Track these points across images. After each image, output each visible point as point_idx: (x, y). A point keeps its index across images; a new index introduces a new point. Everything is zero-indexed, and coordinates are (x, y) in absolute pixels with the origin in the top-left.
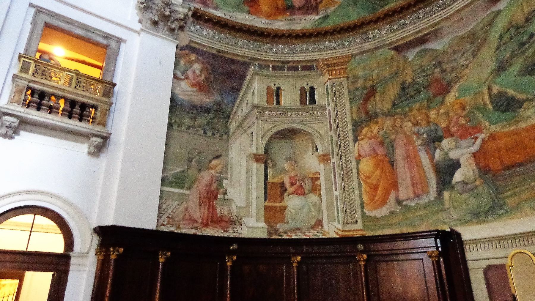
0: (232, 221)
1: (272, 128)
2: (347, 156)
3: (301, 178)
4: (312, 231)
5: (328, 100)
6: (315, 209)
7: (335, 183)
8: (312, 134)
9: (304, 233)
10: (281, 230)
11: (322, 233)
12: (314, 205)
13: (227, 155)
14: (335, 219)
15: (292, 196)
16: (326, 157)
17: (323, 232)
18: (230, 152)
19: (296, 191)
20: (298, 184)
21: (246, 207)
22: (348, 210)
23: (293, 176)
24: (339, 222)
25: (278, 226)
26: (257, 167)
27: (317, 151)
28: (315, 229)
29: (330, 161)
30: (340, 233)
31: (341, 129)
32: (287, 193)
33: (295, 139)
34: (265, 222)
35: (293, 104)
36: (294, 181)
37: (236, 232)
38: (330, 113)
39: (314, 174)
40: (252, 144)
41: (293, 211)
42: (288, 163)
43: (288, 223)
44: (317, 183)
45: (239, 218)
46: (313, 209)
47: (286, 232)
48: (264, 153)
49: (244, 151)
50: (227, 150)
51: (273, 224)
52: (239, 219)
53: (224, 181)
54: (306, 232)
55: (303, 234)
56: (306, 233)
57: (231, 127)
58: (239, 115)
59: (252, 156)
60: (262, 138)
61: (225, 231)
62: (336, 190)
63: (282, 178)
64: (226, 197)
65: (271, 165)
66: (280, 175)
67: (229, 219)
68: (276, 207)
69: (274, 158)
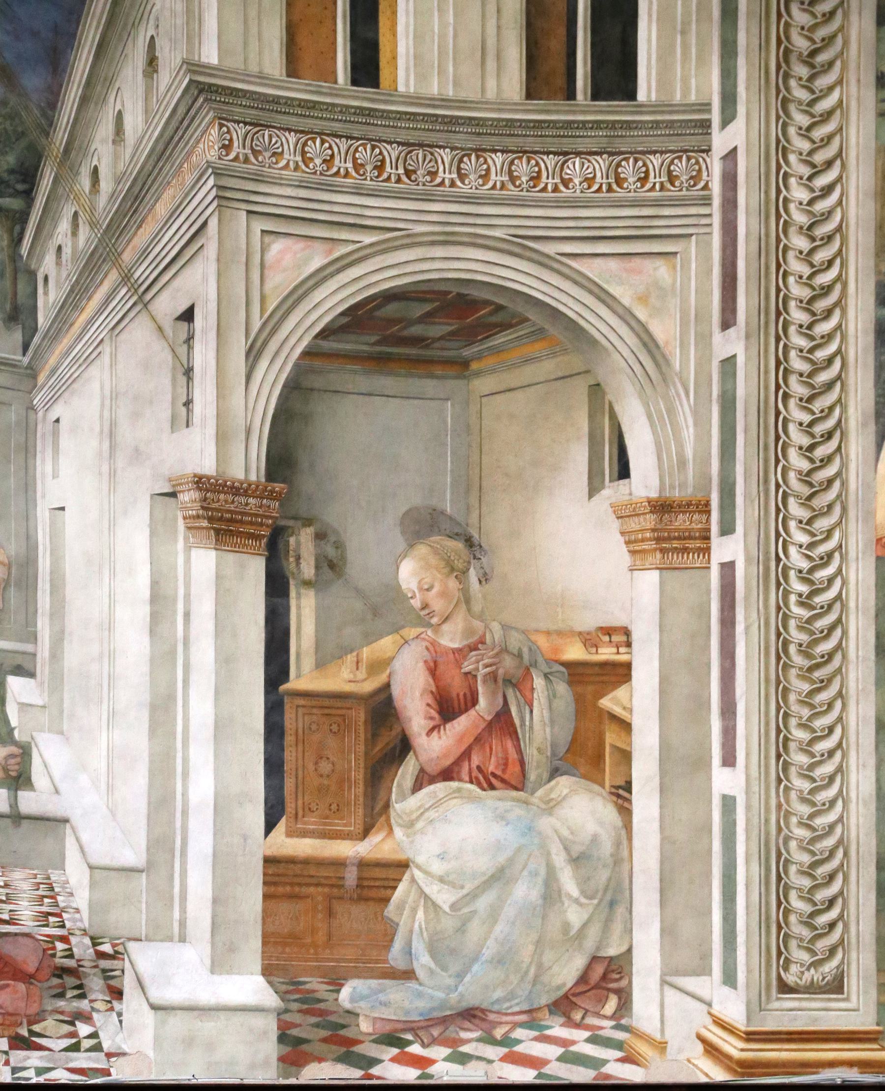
0: (62, 972)
1: (320, 277)
2: (823, 524)
3: (508, 662)
4: (558, 1031)
5: (728, 75)
6: (583, 882)
7: (728, 710)
8: (594, 342)
9: (506, 1041)
10: (365, 1026)
11: (619, 1045)
12: (577, 860)
13: (28, 487)
14: (706, 957)
15: (440, 788)
16: (681, 522)
17: (620, 1035)
18: (43, 465)
19: (466, 754)
20: (484, 706)
21: (149, 868)
22: (796, 903)
23: (454, 651)
24: (729, 979)
25: (345, 994)
26: (219, 577)
27: (624, 472)
28: (577, 1016)
29: (707, 550)
30: (733, 1047)
31: (798, 316)
32: (408, 770)
33: (478, 374)
34: (267, 972)
35: (470, 93)
36: (457, 687)
37: (92, 1042)
38: (730, 180)
39: (589, 640)
40: (188, 403)
41: (444, 897)
42: (422, 549)
43: (409, 975)
44: (606, 703)
45: (107, 948)
46: (569, 883)
47: (391, 1039)
48: (270, 476)
49: (137, 455)
50: (28, 451)
51: (315, 984)
52: (102, 955)
53: (14, 683)
54: (519, 1033)
55: (502, 1051)
56: (518, 1042)
57: (47, 265)
58: (95, 162)
59: (189, 497)
60: (253, 354)
61: (19, 1043)
62: (729, 761)
63: (378, 665)
64: (28, 802)
65: (308, 570)
66: (370, 638)
67: (48, 952)
68: (339, 864)
69: (331, 515)
